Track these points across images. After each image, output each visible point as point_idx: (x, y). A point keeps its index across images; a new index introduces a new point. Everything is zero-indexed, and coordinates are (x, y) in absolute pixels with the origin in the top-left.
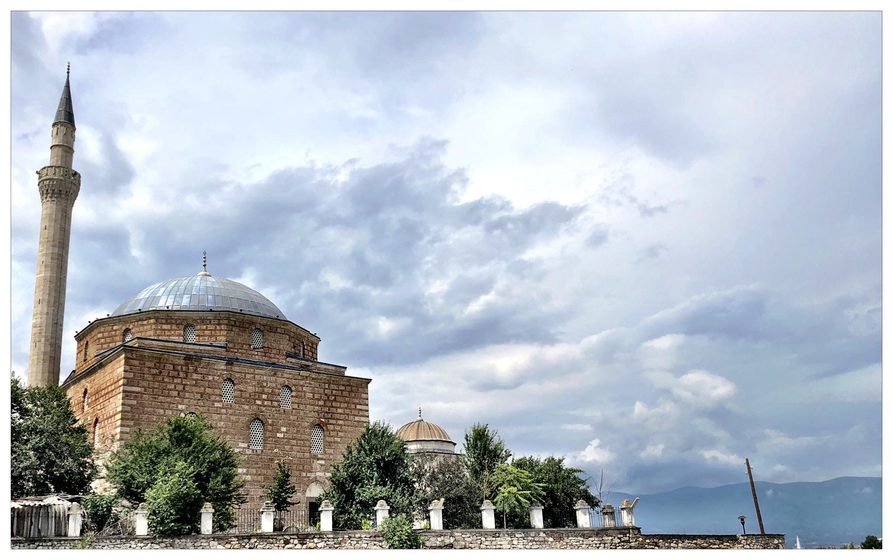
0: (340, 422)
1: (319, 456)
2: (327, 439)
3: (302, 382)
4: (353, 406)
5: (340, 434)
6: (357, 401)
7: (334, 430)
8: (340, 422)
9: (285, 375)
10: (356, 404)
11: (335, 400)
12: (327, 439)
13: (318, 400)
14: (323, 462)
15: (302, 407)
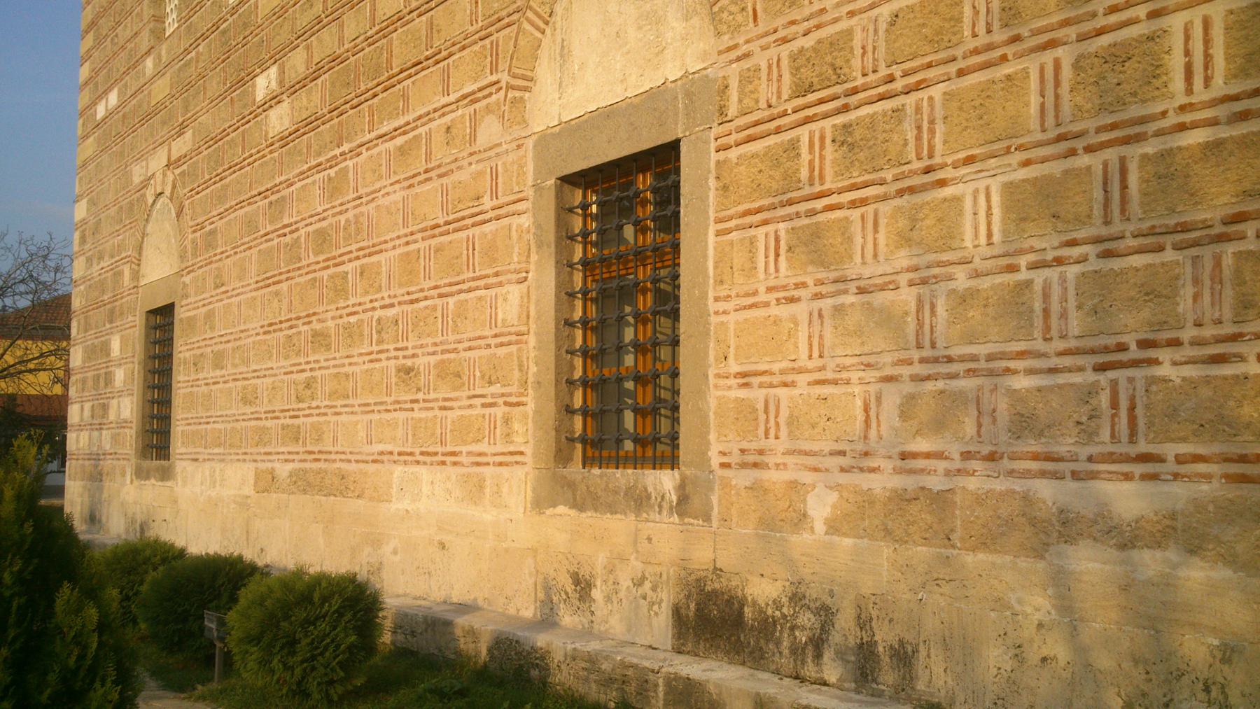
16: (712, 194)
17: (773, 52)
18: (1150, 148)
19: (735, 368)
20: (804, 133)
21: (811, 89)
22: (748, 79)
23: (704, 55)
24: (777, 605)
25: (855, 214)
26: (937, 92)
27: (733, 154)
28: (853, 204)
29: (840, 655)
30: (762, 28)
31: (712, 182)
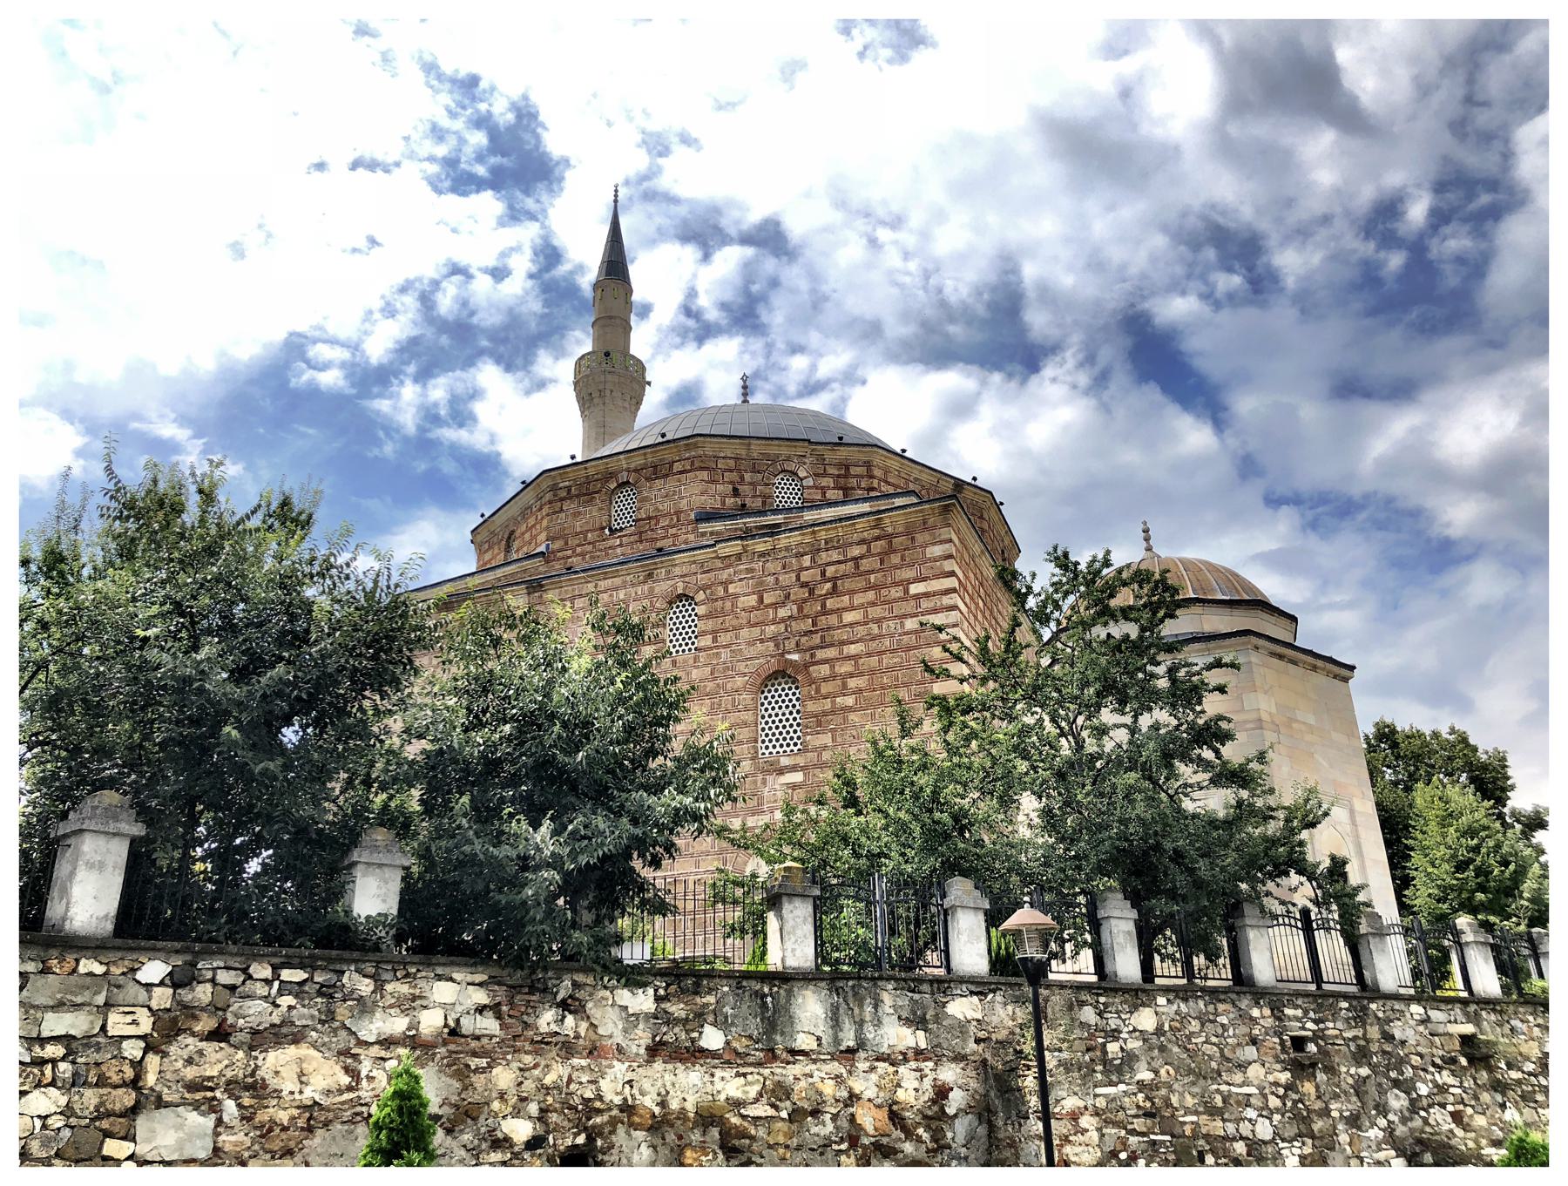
0: (853, 649)
1: (785, 761)
2: (811, 707)
3: (724, 575)
4: (896, 592)
5: (853, 683)
6: (908, 574)
7: (833, 677)
8: (853, 649)
9: (677, 571)
11: (834, 591)
12: (811, 707)
13: (775, 606)
14: (798, 777)
15: (724, 638)
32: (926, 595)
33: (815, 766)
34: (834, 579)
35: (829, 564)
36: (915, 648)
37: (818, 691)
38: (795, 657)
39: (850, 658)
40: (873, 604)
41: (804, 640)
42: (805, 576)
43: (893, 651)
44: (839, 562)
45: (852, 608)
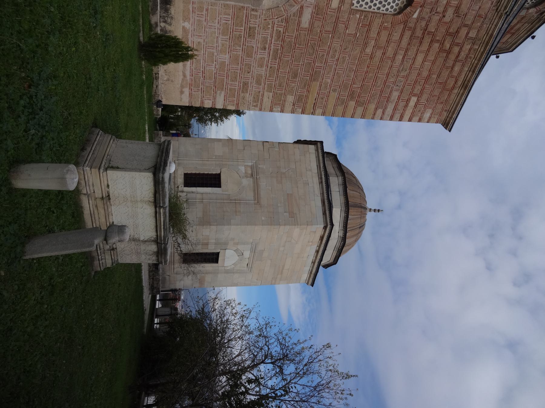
2: (377, 22)
4: (417, 91)
5: (379, 54)
10: (419, 96)
11: (441, 50)
12: (377, 22)
13: (457, 9)
16: (240, 4)
17: (258, 23)
18: (225, 80)
19: (209, 7)
20: (243, 28)
21: (249, 30)
22: (256, 16)
23: (264, 5)
24: (171, 14)
25: (228, 37)
26: (241, 53)
27: (245, 12)
28: (230, 37)
29: (165, 27)
30: (263, 21)
31: (242, 5)
32: (406, 106)
33: (338, 18)
34: (449, 52)
35: (461, 49)
36: (381, 95)
37: (386, 28)
38: (415, 16)
39: (395, 54)
40: (419, 74)
41: (423, 24)
42: (464, 31)
43: (385, 82)
44: (457, 57)
45: (424, 61)
